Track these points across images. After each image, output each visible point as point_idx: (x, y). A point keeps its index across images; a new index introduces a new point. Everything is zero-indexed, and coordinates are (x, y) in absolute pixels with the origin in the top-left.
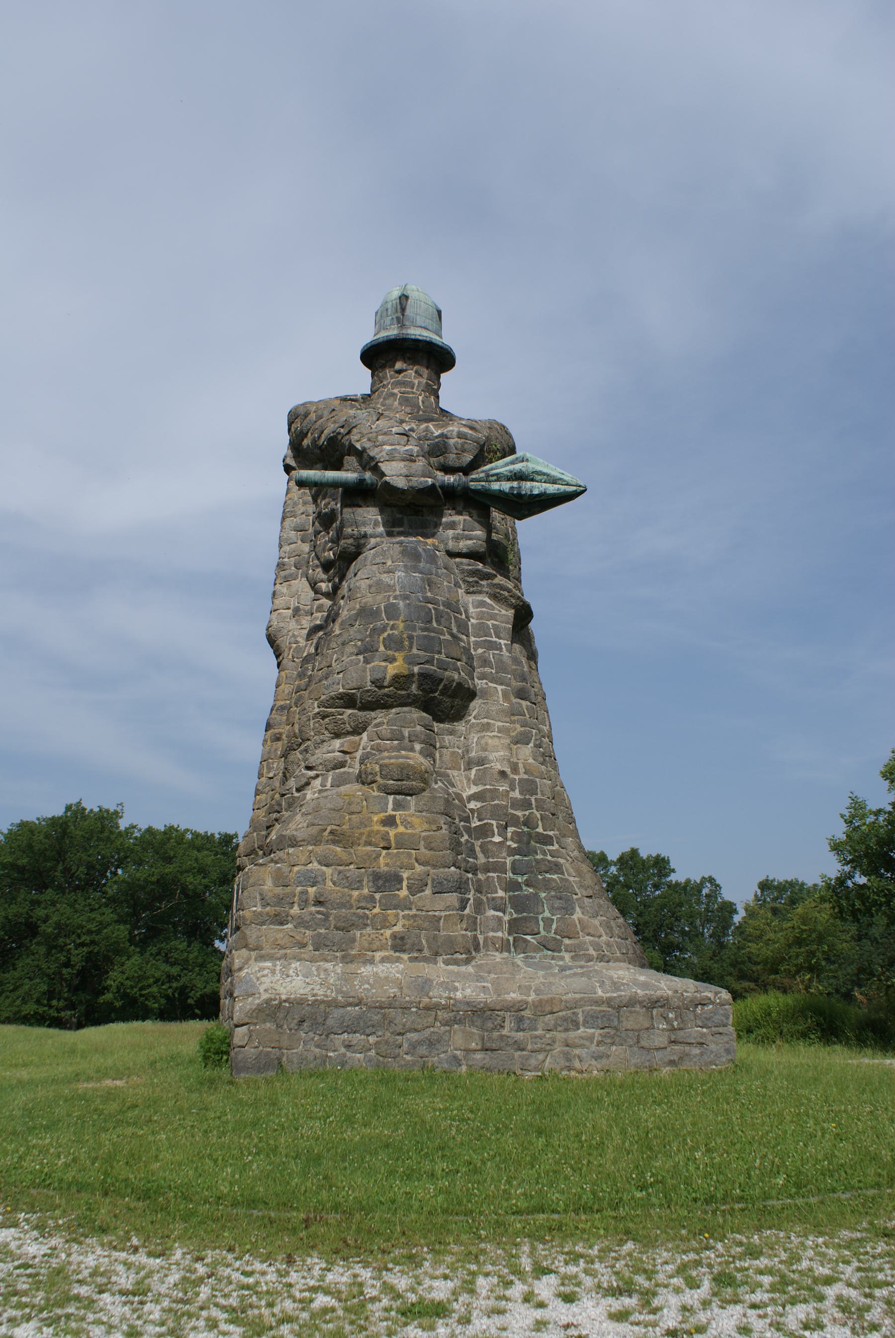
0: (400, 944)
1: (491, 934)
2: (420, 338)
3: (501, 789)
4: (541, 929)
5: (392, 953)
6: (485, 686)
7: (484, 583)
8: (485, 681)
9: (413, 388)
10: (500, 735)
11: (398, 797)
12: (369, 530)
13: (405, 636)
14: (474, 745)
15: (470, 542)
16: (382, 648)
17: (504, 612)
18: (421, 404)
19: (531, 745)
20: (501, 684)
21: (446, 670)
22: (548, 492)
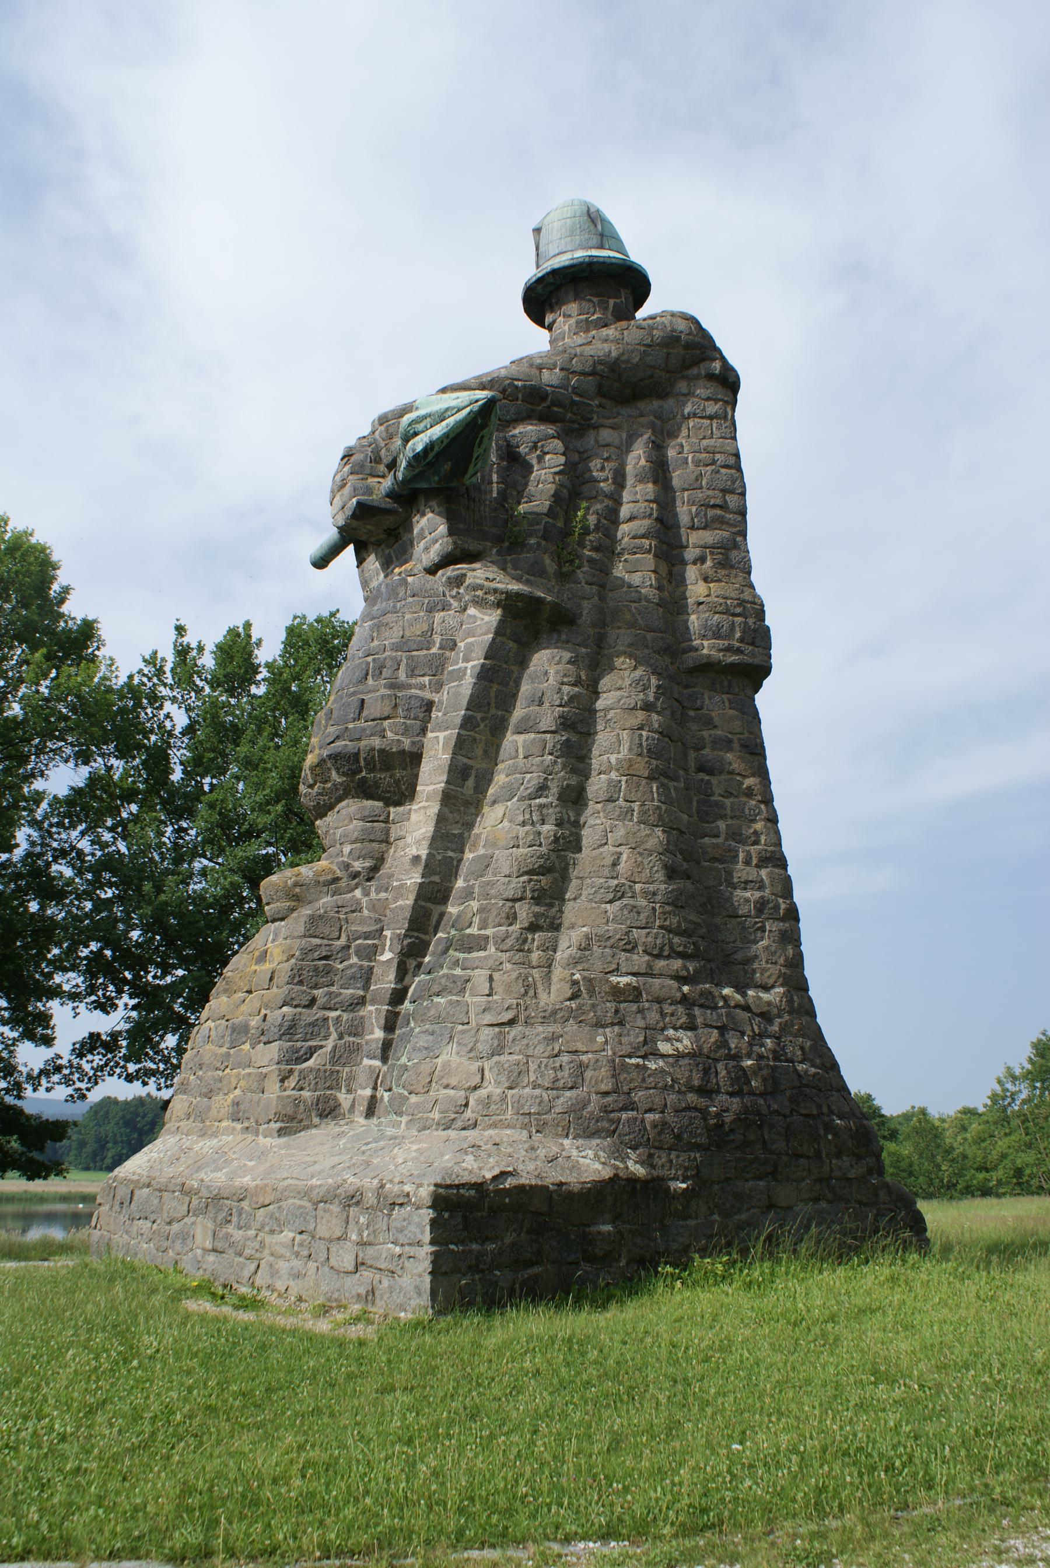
15: (437, 546)
19: (516, 798)
21: (359, 739)
22: (435, 438)
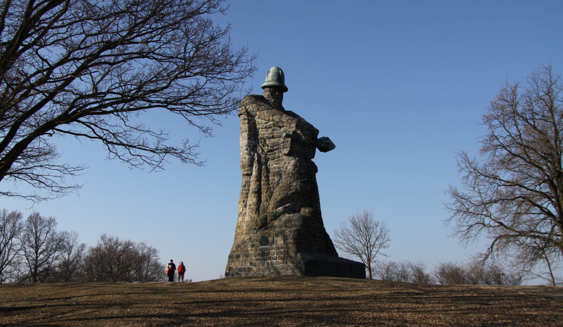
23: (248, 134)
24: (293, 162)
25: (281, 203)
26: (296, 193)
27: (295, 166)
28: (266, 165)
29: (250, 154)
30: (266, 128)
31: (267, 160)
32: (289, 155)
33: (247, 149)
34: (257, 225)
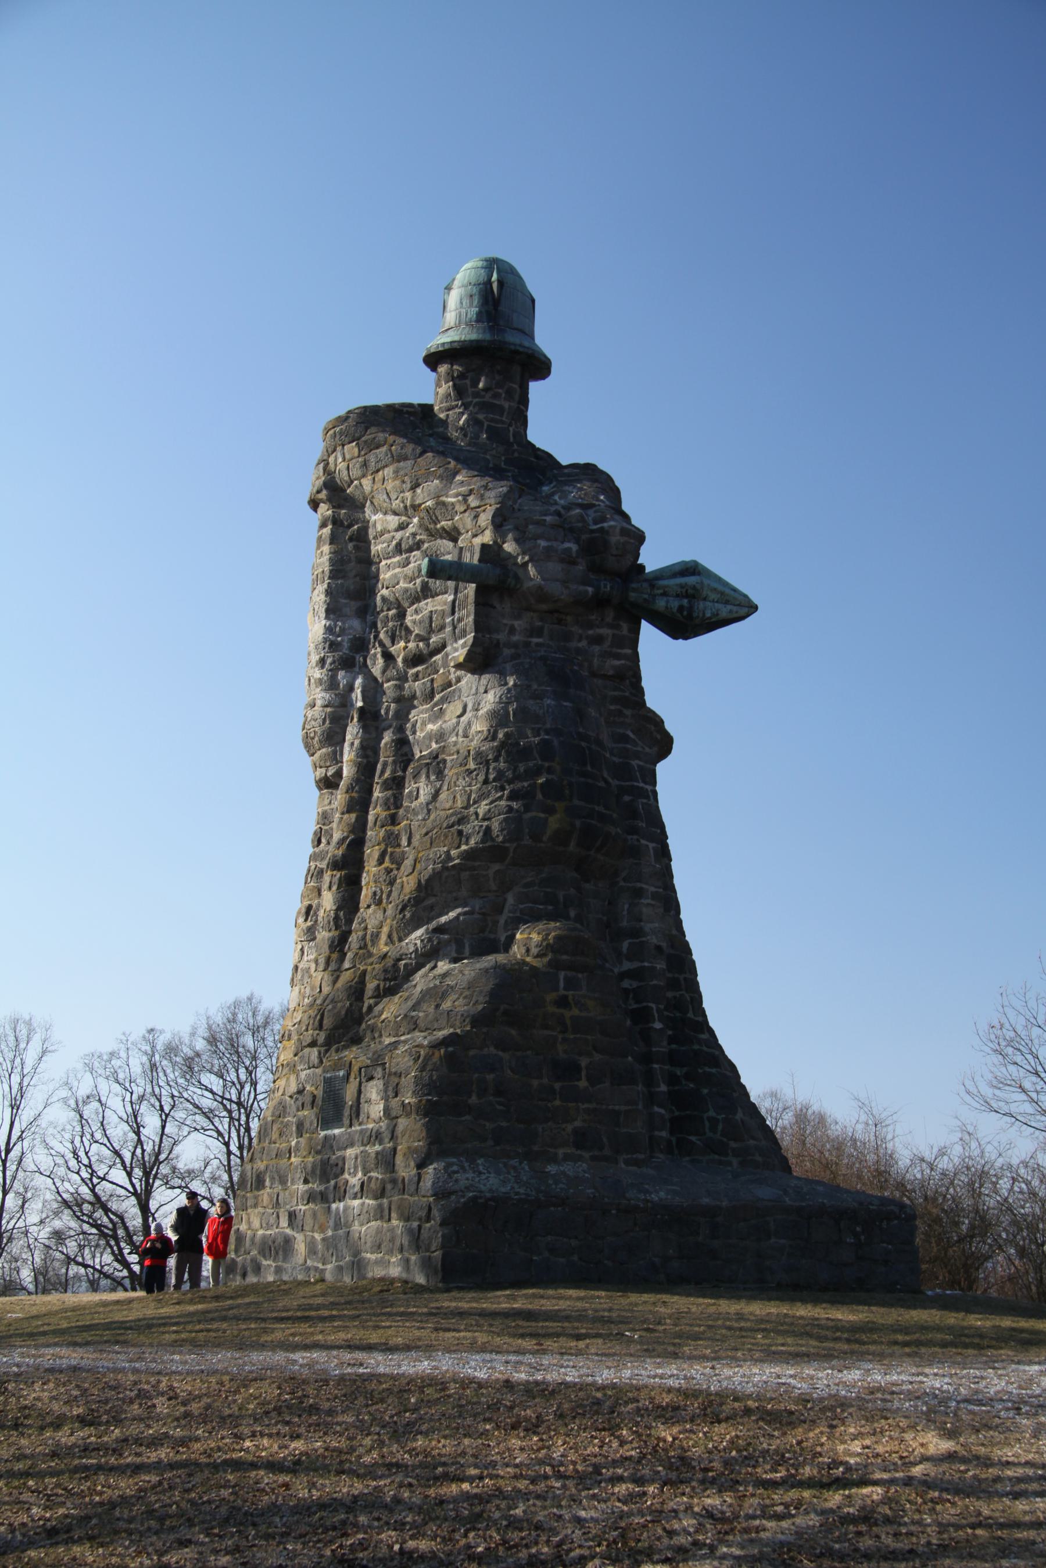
0: (581, 1140)
1: (656, 1133)
2: (521, 349)
3: (658, 966)
4: (707, 1131)
5: (573, 1150)
6: (636, 843)
7: (628, 712)
8: (635, 837)
9: (502, 415)
10: (653, 902)
11: (569, 974)
12: (502, 637)
13: (565, 782)
14: (625, 913)
15: (617, 663)
16: (540, 796)
17: (647, 750)
18: (512, 440)
20: (652, 841)
23: (328, 592)
24: (490, 700)
25: (420, 906)
26: (489, 851)
27: (498, 718)
28: (401, 729)
29: (331, 684)
30: (399, 549)
31: (405, 703)
32: (479, 661)
33: (322, 662)
34: (320, 1027)
